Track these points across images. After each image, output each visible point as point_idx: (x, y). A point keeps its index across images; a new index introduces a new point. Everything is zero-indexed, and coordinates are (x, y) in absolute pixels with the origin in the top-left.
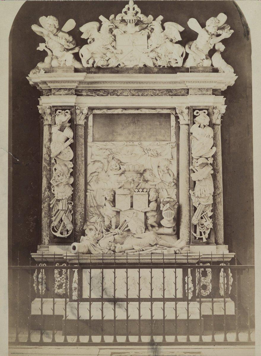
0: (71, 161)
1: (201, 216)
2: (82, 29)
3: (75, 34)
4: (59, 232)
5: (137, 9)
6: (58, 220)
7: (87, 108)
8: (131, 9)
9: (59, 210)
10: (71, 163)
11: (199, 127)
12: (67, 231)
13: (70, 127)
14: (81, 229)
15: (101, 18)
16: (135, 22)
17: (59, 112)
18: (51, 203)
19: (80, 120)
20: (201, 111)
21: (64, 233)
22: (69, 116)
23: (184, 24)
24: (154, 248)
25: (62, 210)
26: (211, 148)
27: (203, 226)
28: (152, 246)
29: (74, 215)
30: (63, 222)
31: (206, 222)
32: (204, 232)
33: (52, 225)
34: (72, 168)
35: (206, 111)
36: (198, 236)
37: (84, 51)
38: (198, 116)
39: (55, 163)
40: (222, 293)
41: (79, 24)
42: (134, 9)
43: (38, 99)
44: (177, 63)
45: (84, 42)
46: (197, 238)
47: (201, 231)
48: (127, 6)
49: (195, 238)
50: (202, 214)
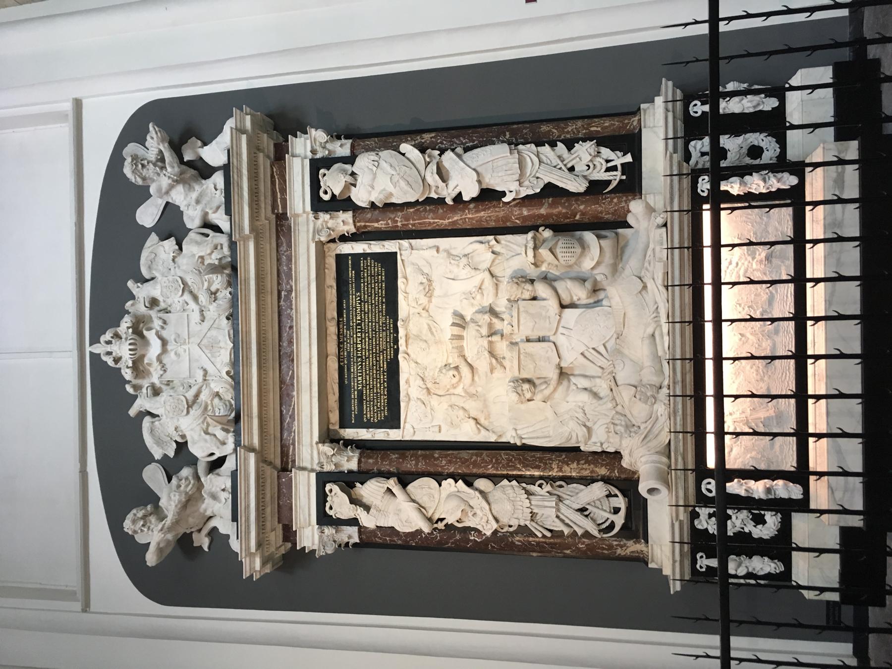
0: (440, 485)
1: (567, 171)
2: (158, 456)
3: (170, 468)
4: (613, 517)
5: (108, 336)
6: (578, 518)
7: (320, 445)
8: (109, 348)
9: (558, 517)
10: (444, 483)
11: (355, 185)
12: (609, 496)
13: (362, 484)
14: (605, 463)
15: (132, 412)
16: (136, 340)
17: (331, 508)
18: (540, 535)
19: (350, 462)
20: (322, 184)
21: (618, 506)
22: (336, 488)
23: (145, 233)
24: (650, 285)
25: (558, 510)
26: (403, 155)
27: (592, 166)
28: (645, 287)
29: (569, 480)
30: (587, 507)
31: (580, 159)
32: (608, 161)
33: (595, 532)
34: (456, 483)
35: (322, 171)
36: (617, 177)
37: (200, 449)
38: (332, 190)
39: (444, 522)
40: (770, 104)
41: (150, 459)
42: (109, 343)
43: (307, 552)
44: (222, 245)
45: (182, 447)
46: (624, 177)
47: (604, 169)
48: (104, 358)
49: (621, 181)
50: (560, 169)
